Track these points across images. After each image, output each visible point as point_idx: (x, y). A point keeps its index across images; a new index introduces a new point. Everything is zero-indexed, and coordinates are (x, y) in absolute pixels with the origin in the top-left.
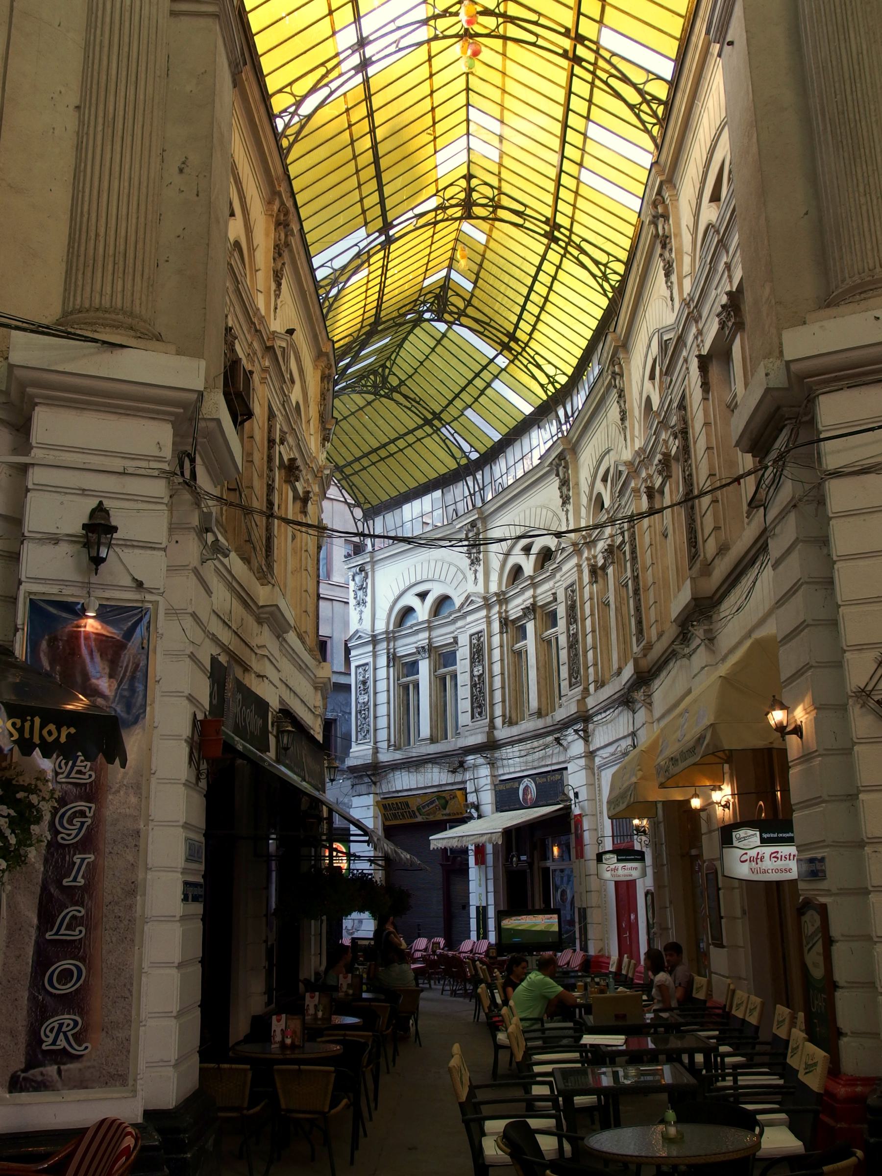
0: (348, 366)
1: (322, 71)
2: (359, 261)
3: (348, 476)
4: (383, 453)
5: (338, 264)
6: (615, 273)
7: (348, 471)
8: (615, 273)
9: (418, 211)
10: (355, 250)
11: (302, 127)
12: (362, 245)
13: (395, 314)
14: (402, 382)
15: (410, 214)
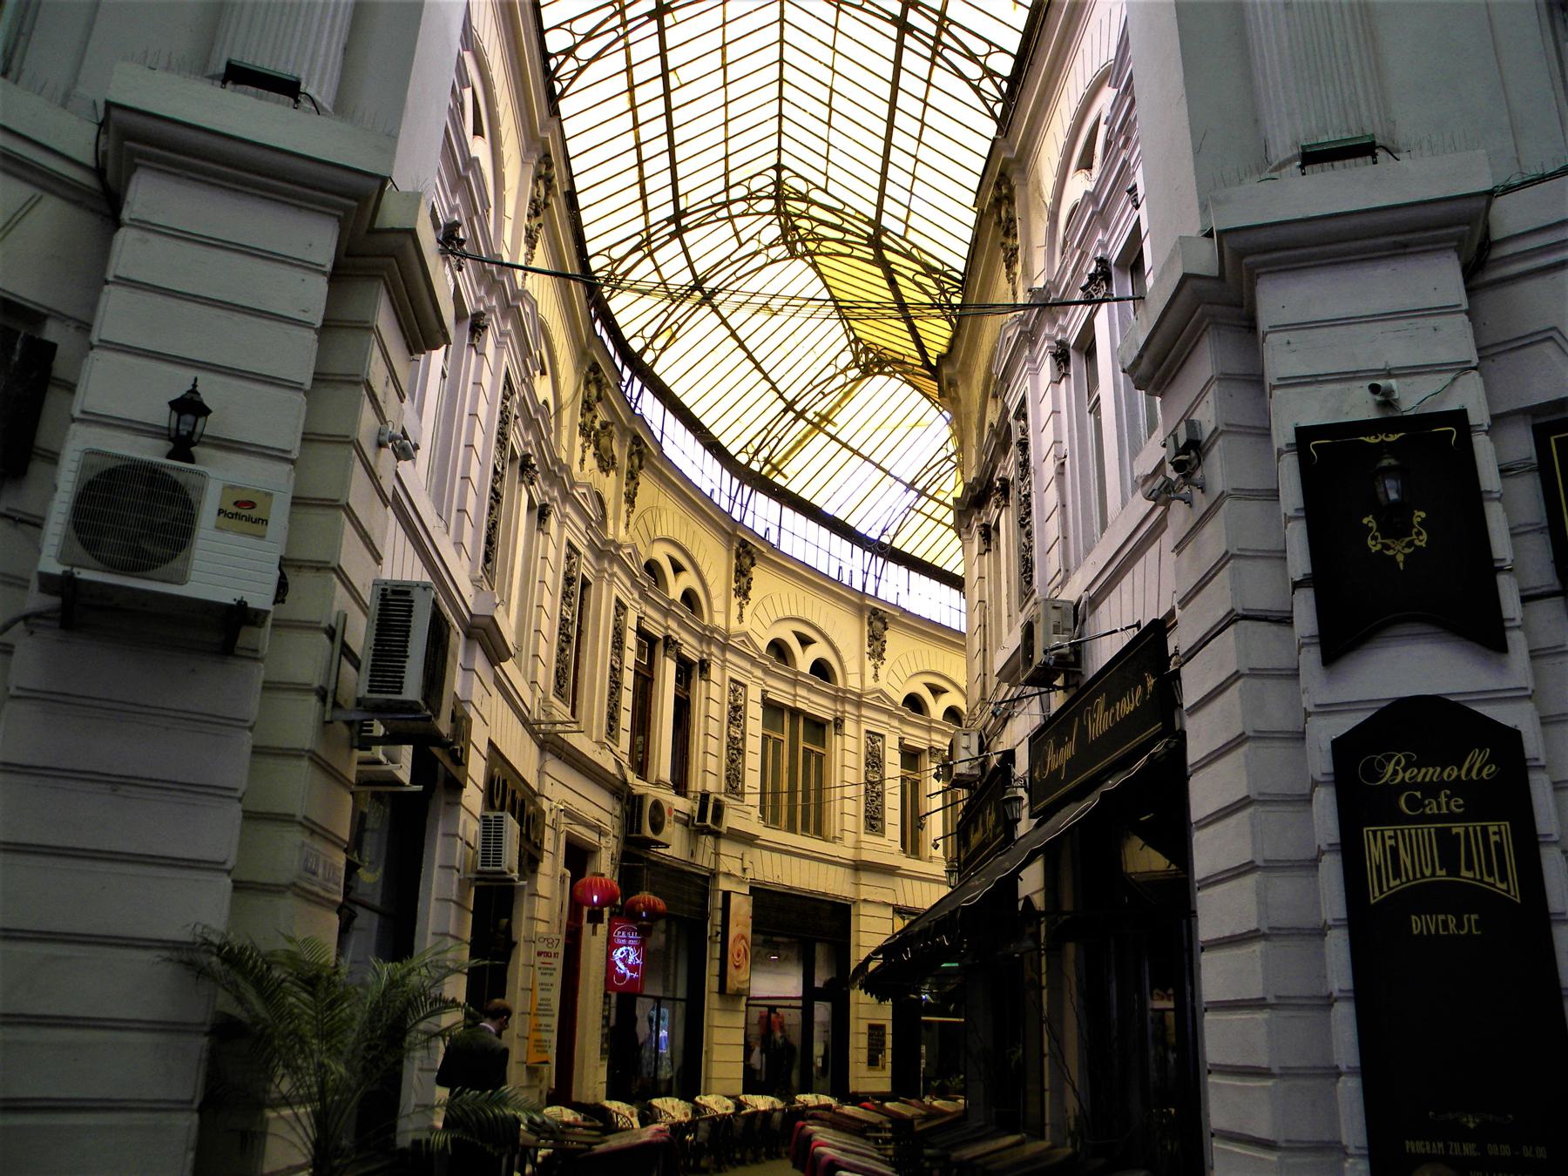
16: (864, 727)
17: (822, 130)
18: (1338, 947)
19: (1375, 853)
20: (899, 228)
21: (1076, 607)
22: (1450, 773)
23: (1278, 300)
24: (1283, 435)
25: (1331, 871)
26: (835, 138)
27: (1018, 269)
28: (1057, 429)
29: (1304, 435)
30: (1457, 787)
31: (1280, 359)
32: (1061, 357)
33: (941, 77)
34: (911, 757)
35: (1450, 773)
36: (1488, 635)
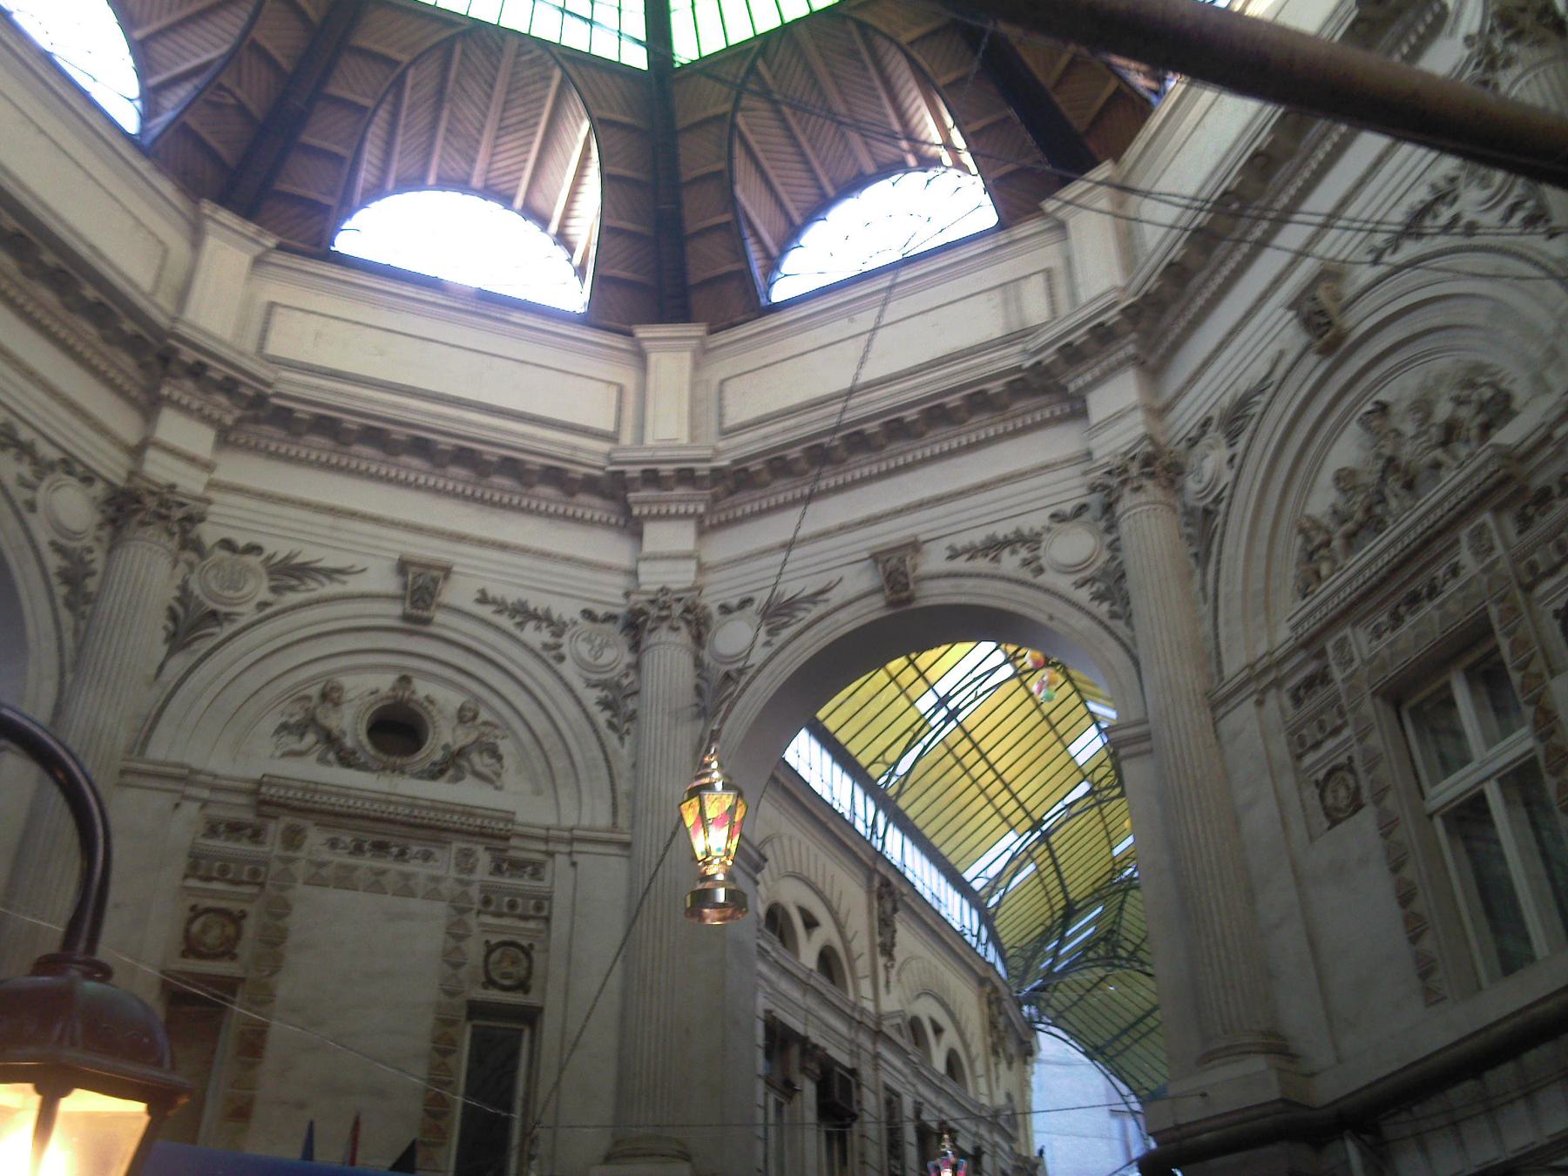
0: (1058, 948)
1: (910, 735)
2: (1016, 863)
3: (1112, 1058)
4: (1142, 1028)
5: (992, 872)
6: (1335, 798)
7: (1110, 1051)
8: (1335, 798)
9: (1068, 800)
10: (1008, 855)
11: (902, 786)
12: (1015, 848)
13: (1090, 890)
14: (1138, 947)
15: (1060, 806)
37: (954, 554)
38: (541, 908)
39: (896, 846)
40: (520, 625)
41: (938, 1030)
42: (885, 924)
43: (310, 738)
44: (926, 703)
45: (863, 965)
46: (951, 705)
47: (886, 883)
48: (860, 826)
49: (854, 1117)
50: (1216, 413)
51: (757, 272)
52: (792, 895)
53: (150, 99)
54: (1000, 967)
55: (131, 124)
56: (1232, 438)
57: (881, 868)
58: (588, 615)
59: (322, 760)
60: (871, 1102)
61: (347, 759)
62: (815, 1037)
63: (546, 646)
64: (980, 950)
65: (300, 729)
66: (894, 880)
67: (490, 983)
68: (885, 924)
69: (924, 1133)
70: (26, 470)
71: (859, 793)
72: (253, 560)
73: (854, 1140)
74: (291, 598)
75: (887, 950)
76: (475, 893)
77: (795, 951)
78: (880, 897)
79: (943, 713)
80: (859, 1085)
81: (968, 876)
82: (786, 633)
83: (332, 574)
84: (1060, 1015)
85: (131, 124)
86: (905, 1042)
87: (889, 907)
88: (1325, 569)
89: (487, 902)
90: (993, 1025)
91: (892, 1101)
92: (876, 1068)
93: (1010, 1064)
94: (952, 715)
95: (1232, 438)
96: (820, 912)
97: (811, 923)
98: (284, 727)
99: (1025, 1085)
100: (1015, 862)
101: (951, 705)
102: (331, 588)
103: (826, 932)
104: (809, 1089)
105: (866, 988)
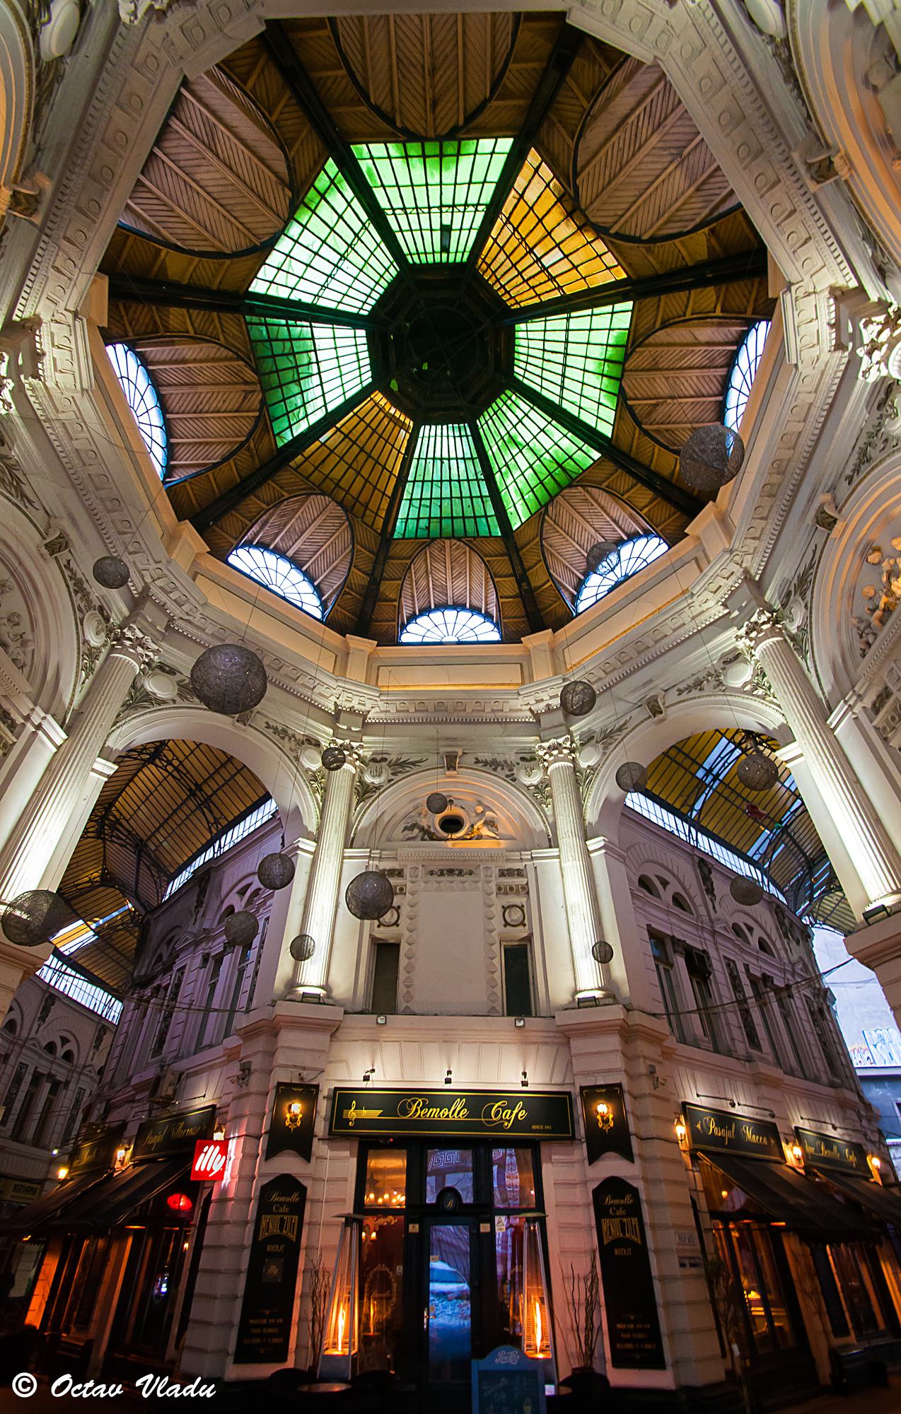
16: (20, 1060)
17: (139, 803)
18: (246, 1254)
19: (264, 1223)
20: (153, 848)
21: (181, 1075)
22: (288, 1199)
23: (287, 1038)
24: (273, 1084)
25: (250, 1228)
26: (143, 807)
27: (202, 910)
28: (194, 987)
29: (280, 1084)
30: (289, 1204)
31: (280, 1058)
32: (206, 959)
33: (198, 813)
34: (37, 1078)
35: (288, 1199)
36: (306, 1154)
37: (680, 692)
38: (525, 890)
39: (704, 843)
40: (495, 770)
41: (750, 929)
42: (706, 879)
43: (416, 831)
44: (700, 774)
45: (698, 901)
46: (714, 772)
47: (702, 860)
48: (683, 836)
49: (710, 973)
50: (792, 588)
51: (569, 603)
52: (651, 872)
53: (324, 605)
54: (782, 898)
55: (318, 615)
56: (803, 596)
57: (696, 853)
58: (523, 759)
59: (423, 839)
60: (717, 966)
61: (432, 837)
62: (678, 936)
63: (507, 776)
64: (766, 889)
65: (411, 828)
66: (709, 860)
67: (507, 924)
68: (706, 879)
69: (753, 981)
70: (293, 745)
71: (679, 821)
72: (384, 764)
73: (713, 987)
74: (401, 776)
75: (710, 891)
76: (493, 886)
77: (659, 897)
78: (700, 868)
79: (710, 777)
80: (709, 958)
81: (750, 854)
82: (612, 747)
83: (414, 764)
84: (826, 919)
85: (318, 615)
86: (732, 936)
87: (706, 870)
88: (871, 639)
89: (499, 889)
90: (782, 924)
91: (730, 964)
92: (717, 949)
93: (798, 943)
94: (716, 777)
95: (803, 596)
96: (667, 876)
97: (665, 883)
98: (406, 828)
99: (810, 953)
100: (773, 845)
101: (714, 772)
102: (415, 769)
103: (674, 887)
104: (680, 962)
105: (702, 911)
